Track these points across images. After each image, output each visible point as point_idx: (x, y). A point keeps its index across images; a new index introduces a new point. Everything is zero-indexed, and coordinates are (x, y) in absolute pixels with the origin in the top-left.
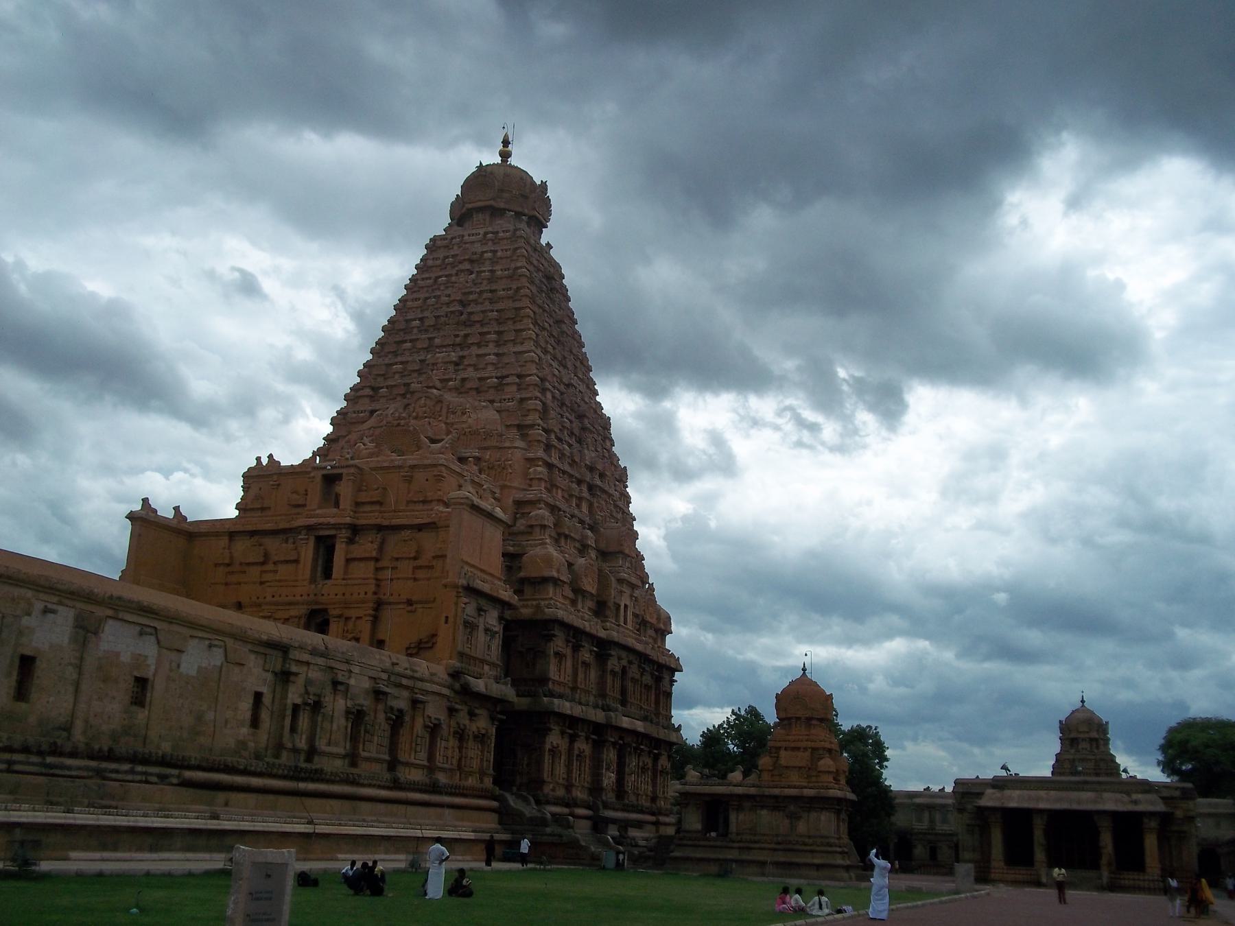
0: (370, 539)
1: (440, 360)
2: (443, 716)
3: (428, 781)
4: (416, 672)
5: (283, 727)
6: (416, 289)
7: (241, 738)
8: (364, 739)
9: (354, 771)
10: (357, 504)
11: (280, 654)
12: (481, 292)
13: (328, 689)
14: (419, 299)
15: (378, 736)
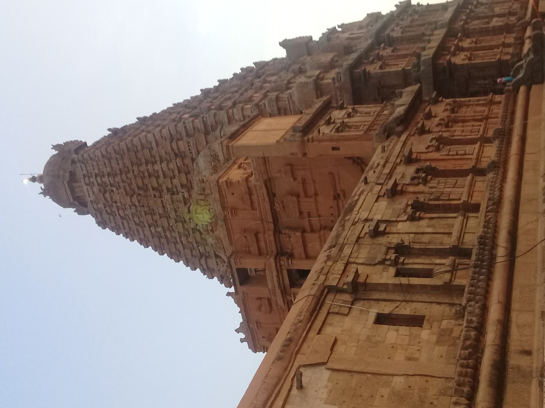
0: (288, 239)
1: (172, 206)
2: (431, 136)
3: (497, 142)
4: (378, 164)
5: (424, 287)
6: (132, 233)
7: (434, 338)
8: (447, 200)
9: (483, 208)
10: (260, 254)
11: (331, 296)
12: (123, 181)
13: (383, 240)
14: (137, 229)
15: (444, 188)
